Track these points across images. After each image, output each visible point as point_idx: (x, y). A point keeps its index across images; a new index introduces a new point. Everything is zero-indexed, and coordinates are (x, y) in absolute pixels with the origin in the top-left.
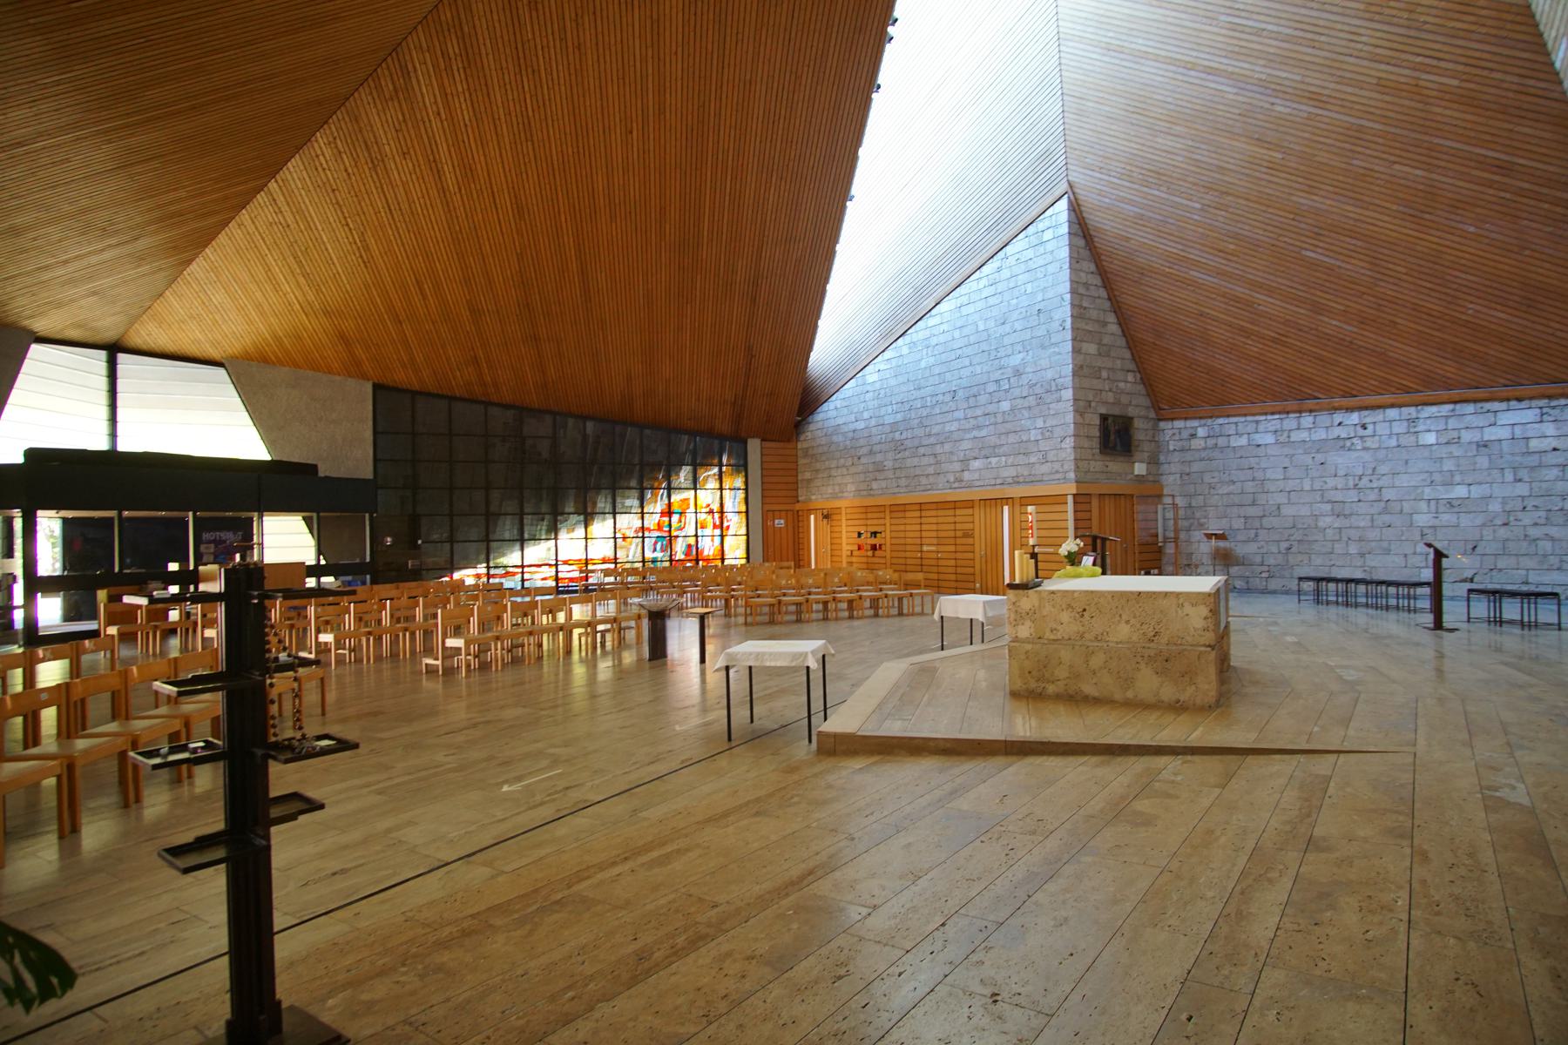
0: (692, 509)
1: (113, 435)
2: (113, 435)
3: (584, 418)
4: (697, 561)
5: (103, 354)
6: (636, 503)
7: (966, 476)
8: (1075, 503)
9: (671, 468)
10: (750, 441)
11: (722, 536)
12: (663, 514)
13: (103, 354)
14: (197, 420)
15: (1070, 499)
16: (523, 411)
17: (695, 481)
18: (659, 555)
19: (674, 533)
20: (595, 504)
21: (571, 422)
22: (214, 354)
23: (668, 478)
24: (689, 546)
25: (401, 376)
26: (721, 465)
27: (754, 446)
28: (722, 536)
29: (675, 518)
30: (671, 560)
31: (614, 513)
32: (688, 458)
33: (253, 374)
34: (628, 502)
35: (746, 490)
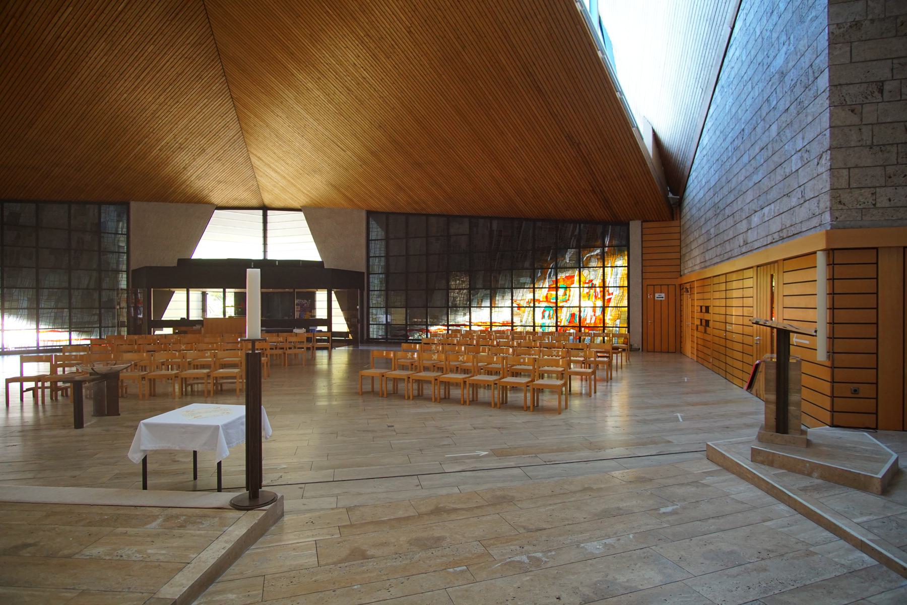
0: (576, 284)
1: (265, 252)
2: (265, 252)
3: (491, 218)
4: (580, 327)
5: (261, 212)
6: (529, 280)
7: (751, 236)
8: (831, 264)
9: (558, 251)
10: (632, 224)
11: (604, 308)
12: (550, 288)
13: (261, 212)
14: (294, 241)
15: (821, 259)
16: (449, 218)
17: (579, 260)
18: (547, 321)
19: (559, 304)
20: (497, 281)
21: (481, 221)
22: (296, 205)
23: (555, 258)
24: (573, 315)
25: (376, 205)
26: (604, 246)
27: (635, 227)
28: (604, 308)
29: (561, 292)
30: (557, 326)
31: (512, 289)
32: (573, 242)
33: (316, 215)
34: (522, 280)
35: (628, 267)
